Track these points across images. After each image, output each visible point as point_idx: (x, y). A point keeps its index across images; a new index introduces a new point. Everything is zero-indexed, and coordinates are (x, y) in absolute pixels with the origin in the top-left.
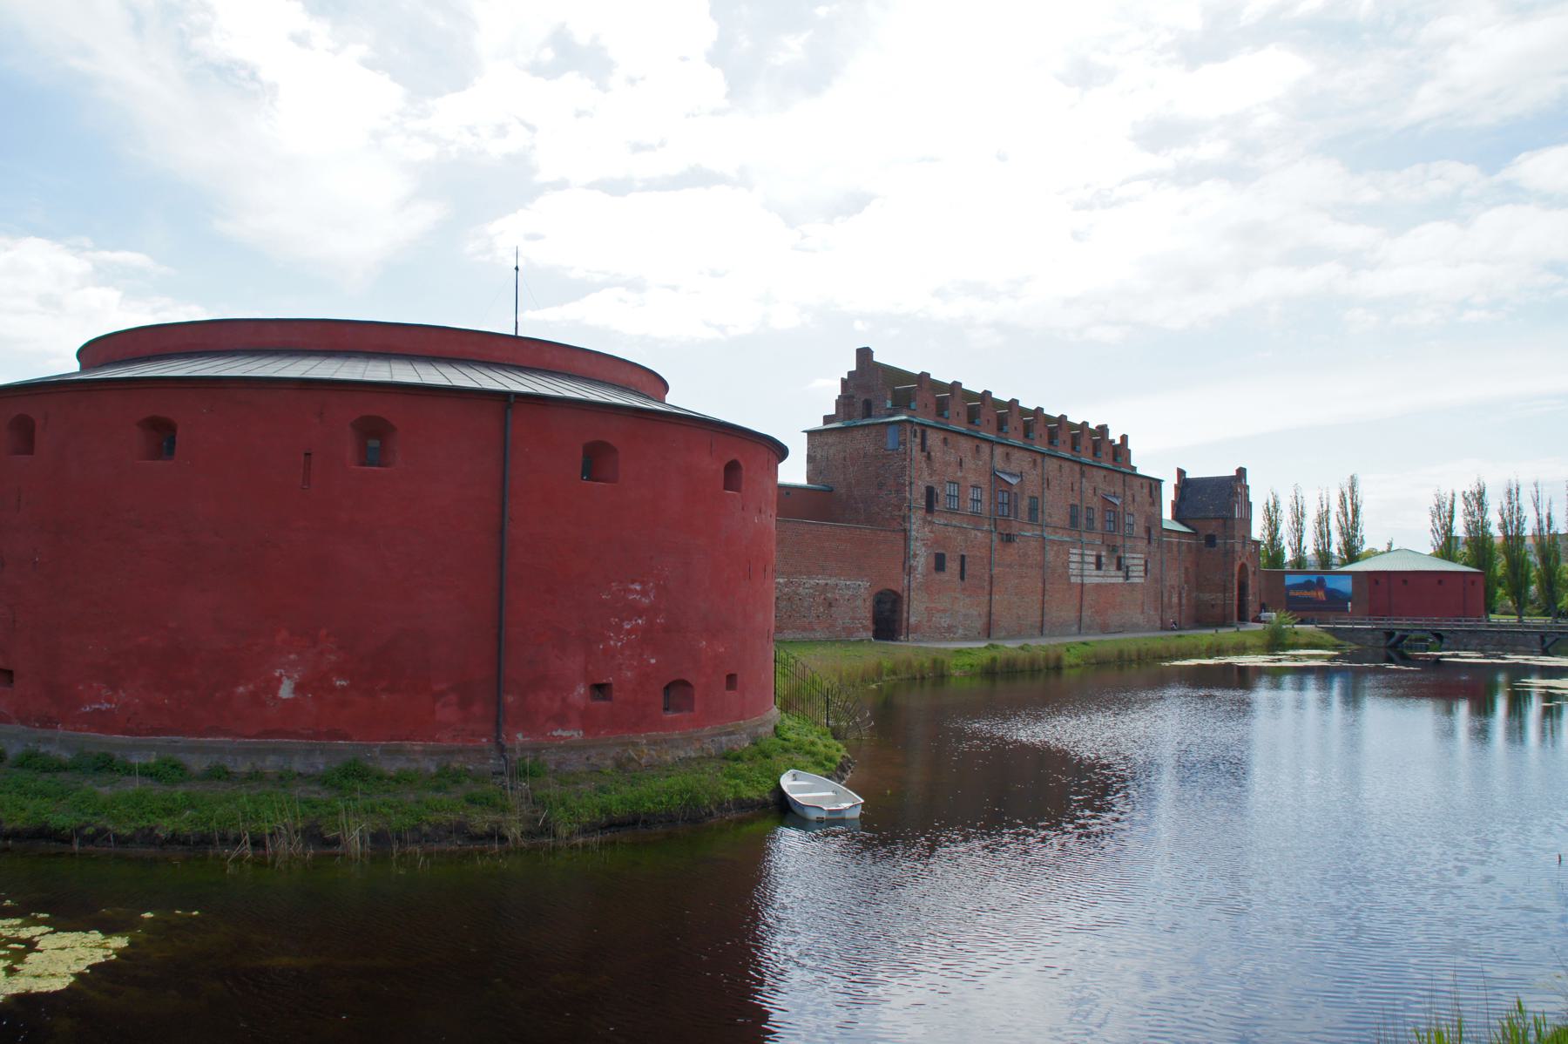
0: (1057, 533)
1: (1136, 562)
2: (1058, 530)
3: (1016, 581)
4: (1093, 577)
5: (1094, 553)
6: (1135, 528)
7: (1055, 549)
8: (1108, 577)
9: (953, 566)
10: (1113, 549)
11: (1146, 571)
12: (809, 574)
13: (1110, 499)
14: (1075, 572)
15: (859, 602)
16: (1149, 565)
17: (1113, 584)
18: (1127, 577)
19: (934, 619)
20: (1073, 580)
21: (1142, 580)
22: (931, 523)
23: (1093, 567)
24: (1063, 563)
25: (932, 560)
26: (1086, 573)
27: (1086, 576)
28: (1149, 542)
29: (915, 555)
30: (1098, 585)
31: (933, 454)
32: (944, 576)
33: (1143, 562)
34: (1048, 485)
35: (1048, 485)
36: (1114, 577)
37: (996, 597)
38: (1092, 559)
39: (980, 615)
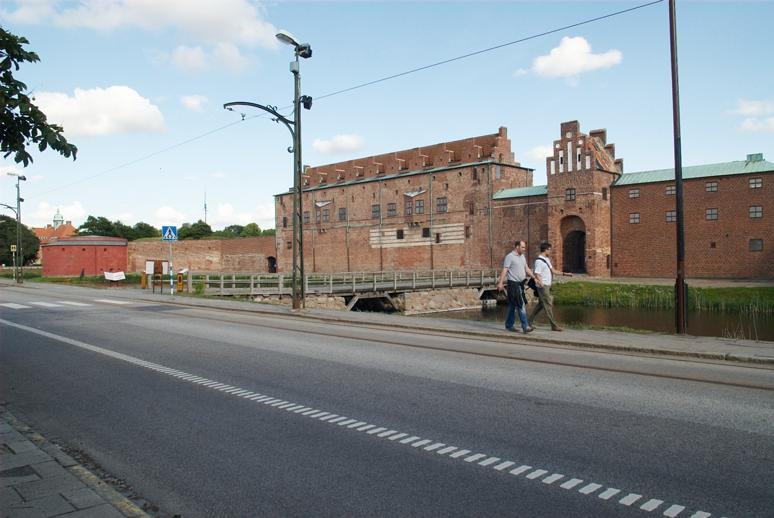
1: (450, 229)
4: (391, 242)
6: (449, 206)
10: (413, 225)
11: (467, 236)
12: (248, 253)
16: (471, 230)
17: (419, 247)
18: (438, 240)
20: (373, 246)
21: (463, 242)
23: (395, 238)
28: (472, 213)
29: (279, 244)
30: (399, 248)
33: (462, 229)
36: (415, 240)
38: (395, 233)
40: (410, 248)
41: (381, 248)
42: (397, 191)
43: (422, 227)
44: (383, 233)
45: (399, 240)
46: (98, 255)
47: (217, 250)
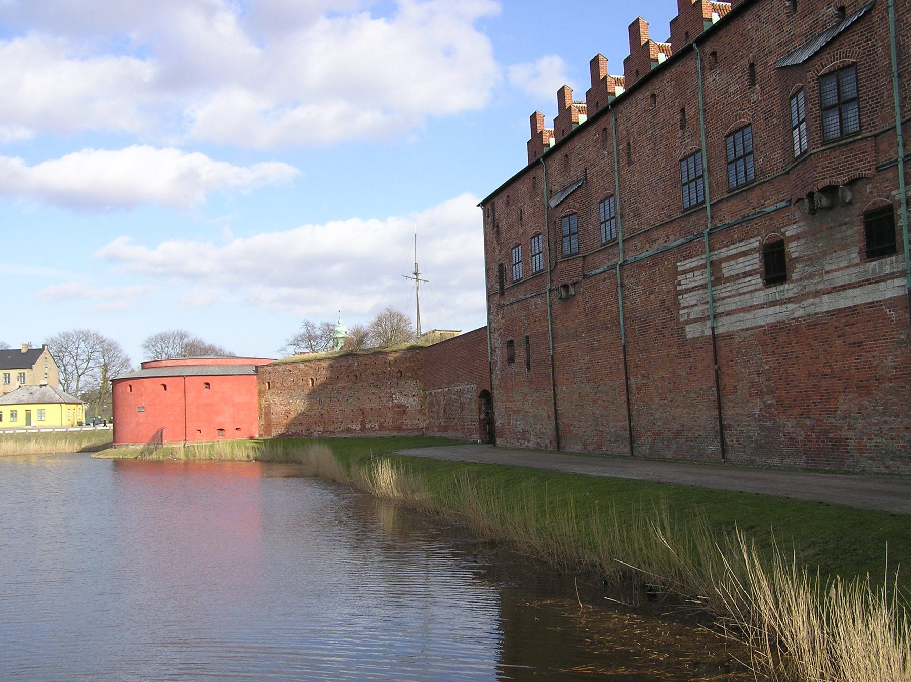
0: (652, 242)
2: (655, 235)
3: (587, 359)
5: (755, 243)
7: (643, 277)
8: (817, 294)
9: (520, 353)
13: (788, 62)
14: (695, 313)
15: (473, 405)
17: (853, 310)
19: (511, 421)
20: (691, 331)
22: (501, 307)
24: (663, 301)
25: (505, 350)
26: (720, 310)
27: (721, 315)
30: (776, 329)
31: (500, 225)
32: (514, 368)
34: (629, 155)
35: (629, 155)
37: (562, 389)
38: (754, 262)
39: (549, 417)
40: (815, 323)
41: (714, 337)
42: (752, 66)
43: (858, 209)
44: (715, 266)
45: (774, 292)
46: (191, 396)
47: (415, 378)
